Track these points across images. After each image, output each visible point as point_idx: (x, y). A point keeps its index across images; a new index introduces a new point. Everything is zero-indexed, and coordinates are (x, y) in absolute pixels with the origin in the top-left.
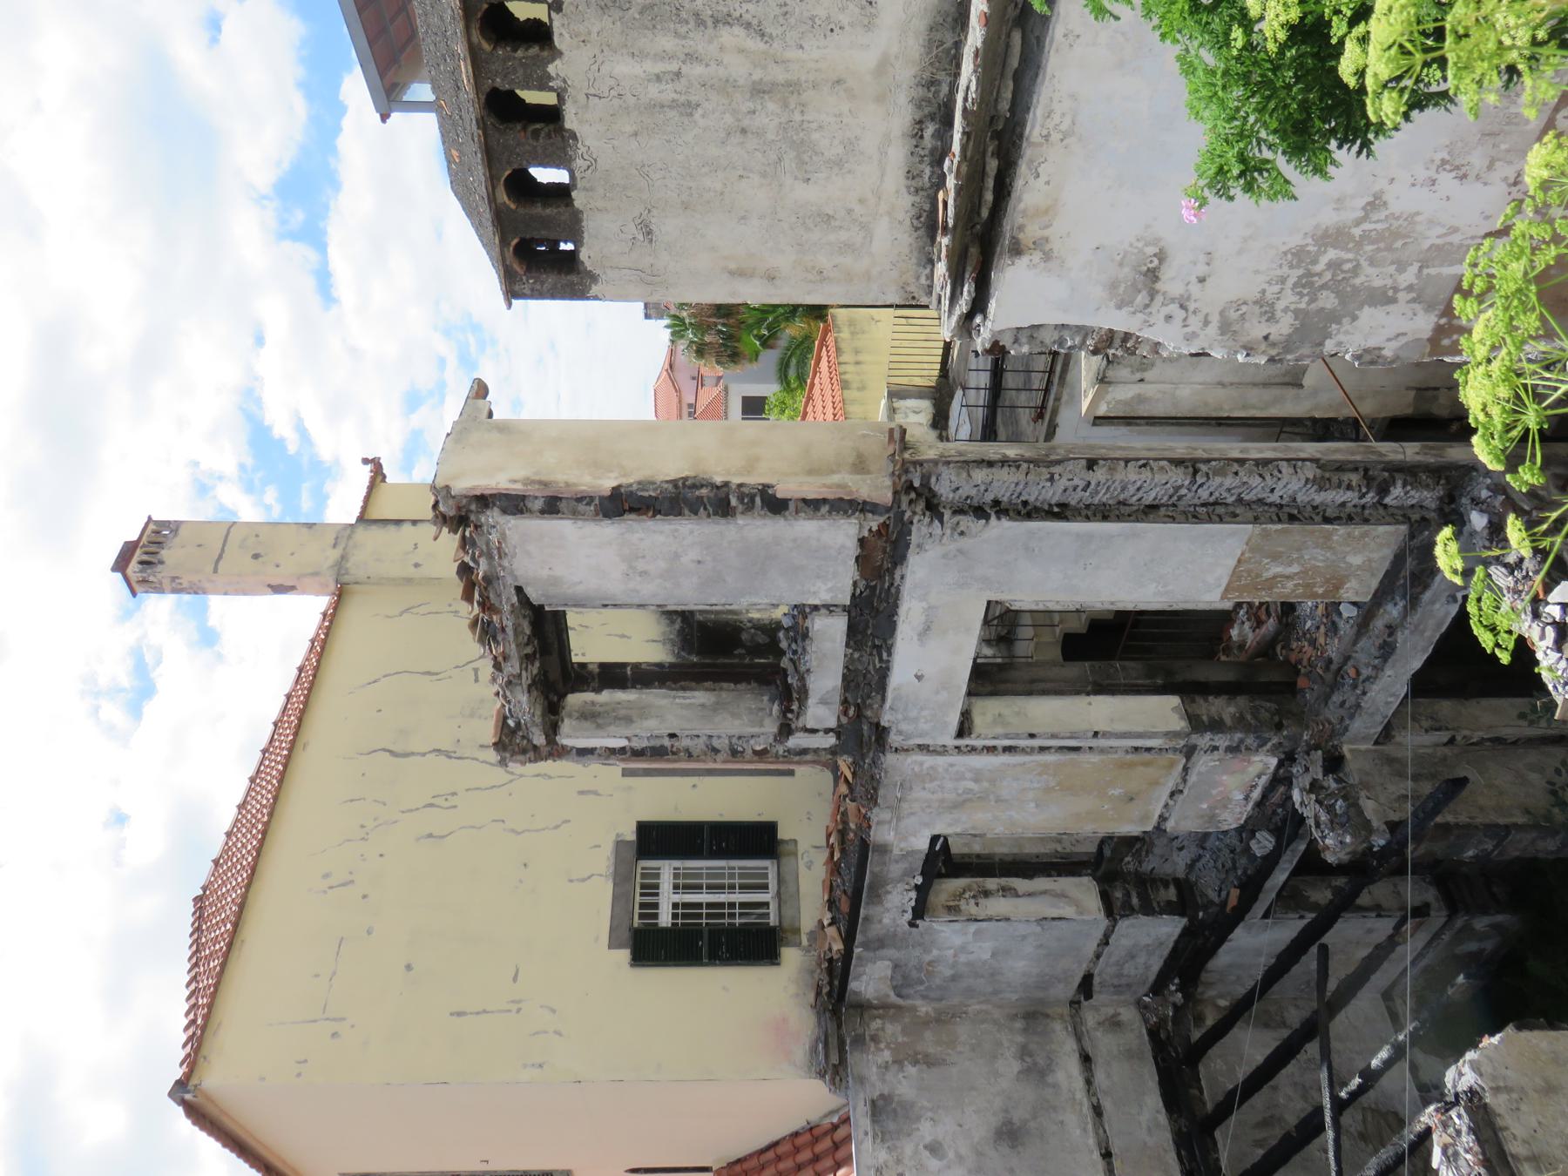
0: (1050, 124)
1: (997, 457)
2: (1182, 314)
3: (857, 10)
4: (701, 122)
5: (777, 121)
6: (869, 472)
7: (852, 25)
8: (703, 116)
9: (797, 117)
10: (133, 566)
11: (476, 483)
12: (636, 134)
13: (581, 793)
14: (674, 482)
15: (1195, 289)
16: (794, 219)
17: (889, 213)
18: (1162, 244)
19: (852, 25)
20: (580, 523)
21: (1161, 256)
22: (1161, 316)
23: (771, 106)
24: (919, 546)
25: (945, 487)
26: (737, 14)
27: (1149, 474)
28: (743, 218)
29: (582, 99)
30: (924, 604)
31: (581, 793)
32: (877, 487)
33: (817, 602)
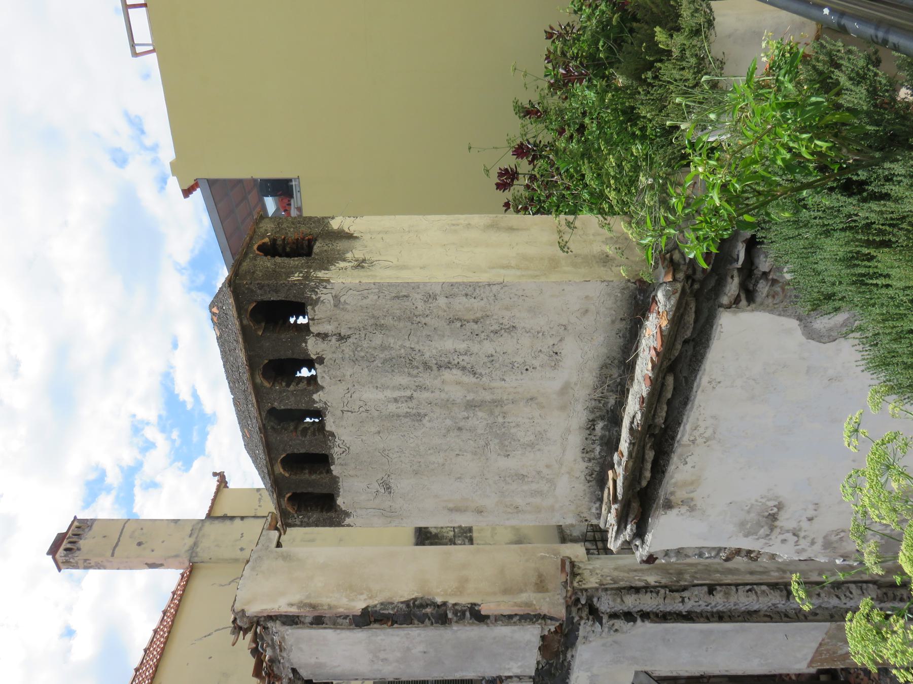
0: (696, 433)
1: (642, 584)
2: (795, 538)
3: (546, 358)
4: (428, 425)
5: (485, 422)
6: (547, 591)
7: (542, 366)
8: (430, 421)
9: (500, 420)
10: (61, 552)
11: (264, 607)
12: (379, 432)
14: (407, 603)
15: (805, 525)
16: (497, 478)
17: (569, 473)
18: (781, 499)
19: (542, 366)
20: (338, 631)
21: (780, 507)
22: (779, 540)
23: (480, 414)
24: (585, 638)
25: (605, 604)
26: (456, 362)
27: (755, 597)
28: (459, 478)
29: (339, 413)
30: (589, 674)
32: (553, 604)
33: (510, 674)
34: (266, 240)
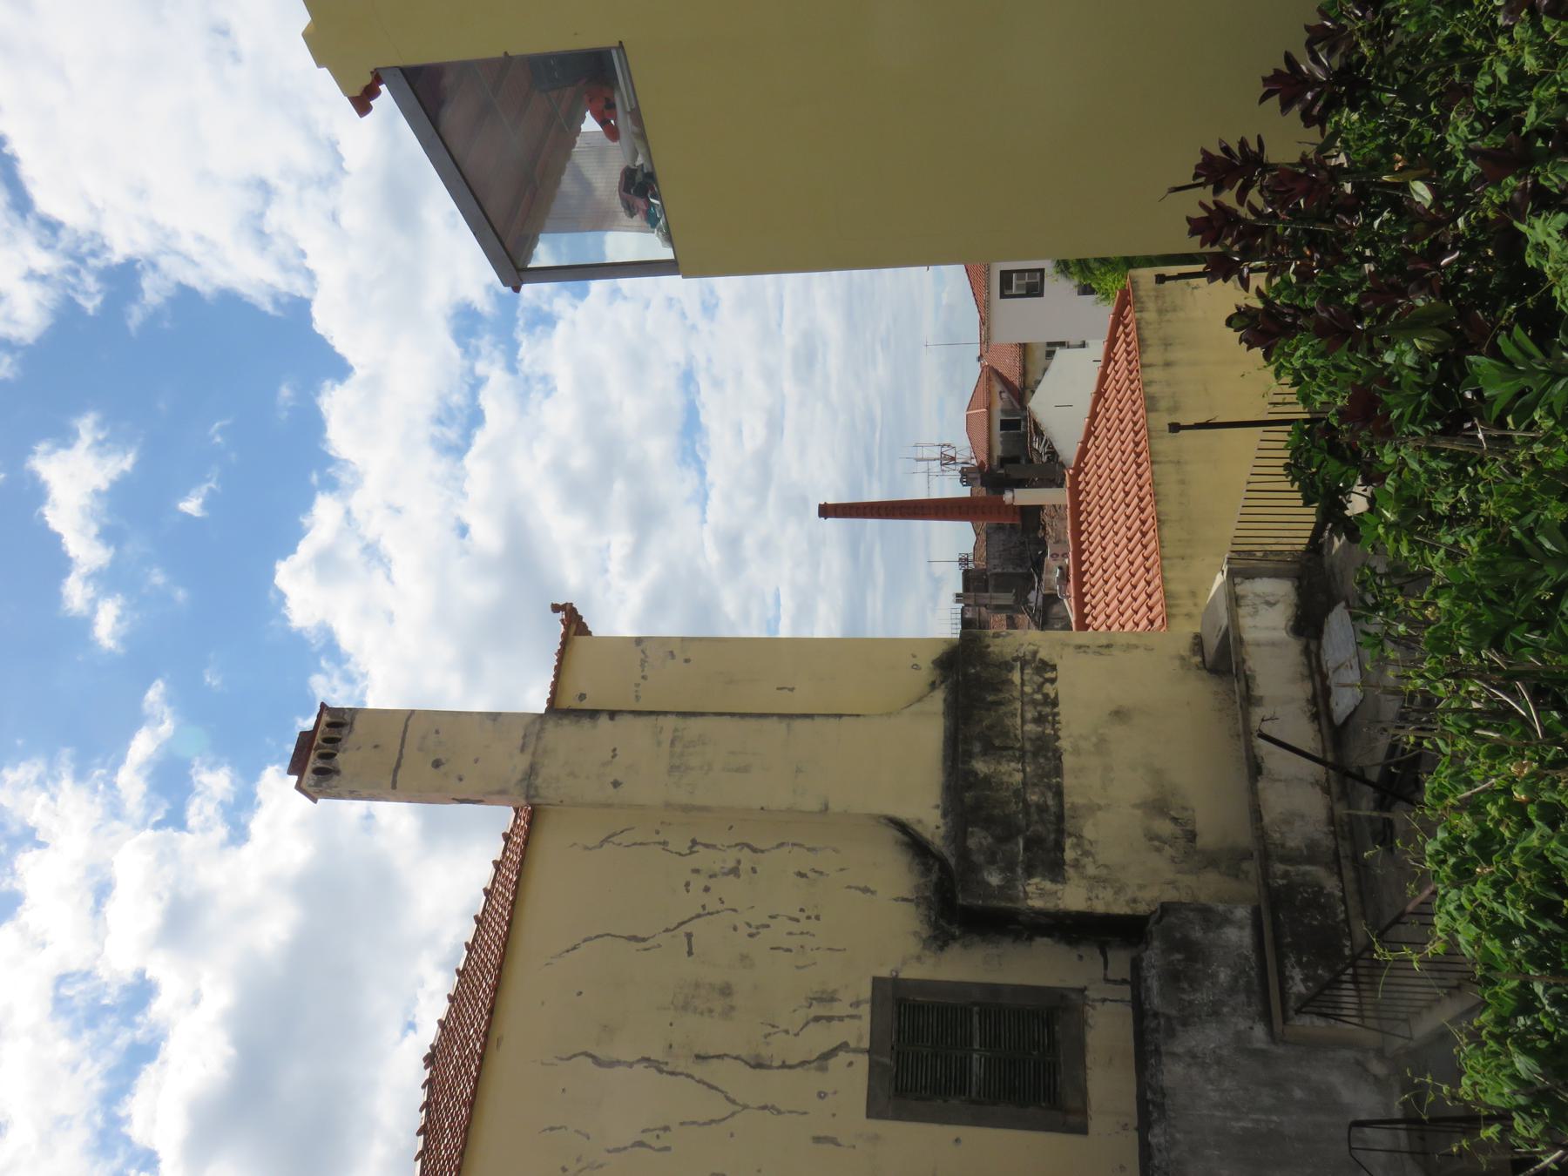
10: (313, 762)
13: (818, 1140)
31: (818, 1140)
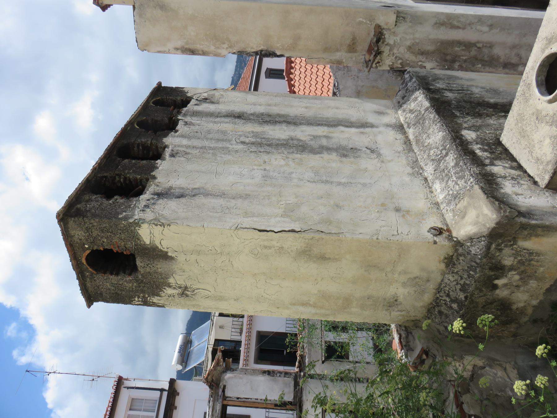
34: (88, 252)
